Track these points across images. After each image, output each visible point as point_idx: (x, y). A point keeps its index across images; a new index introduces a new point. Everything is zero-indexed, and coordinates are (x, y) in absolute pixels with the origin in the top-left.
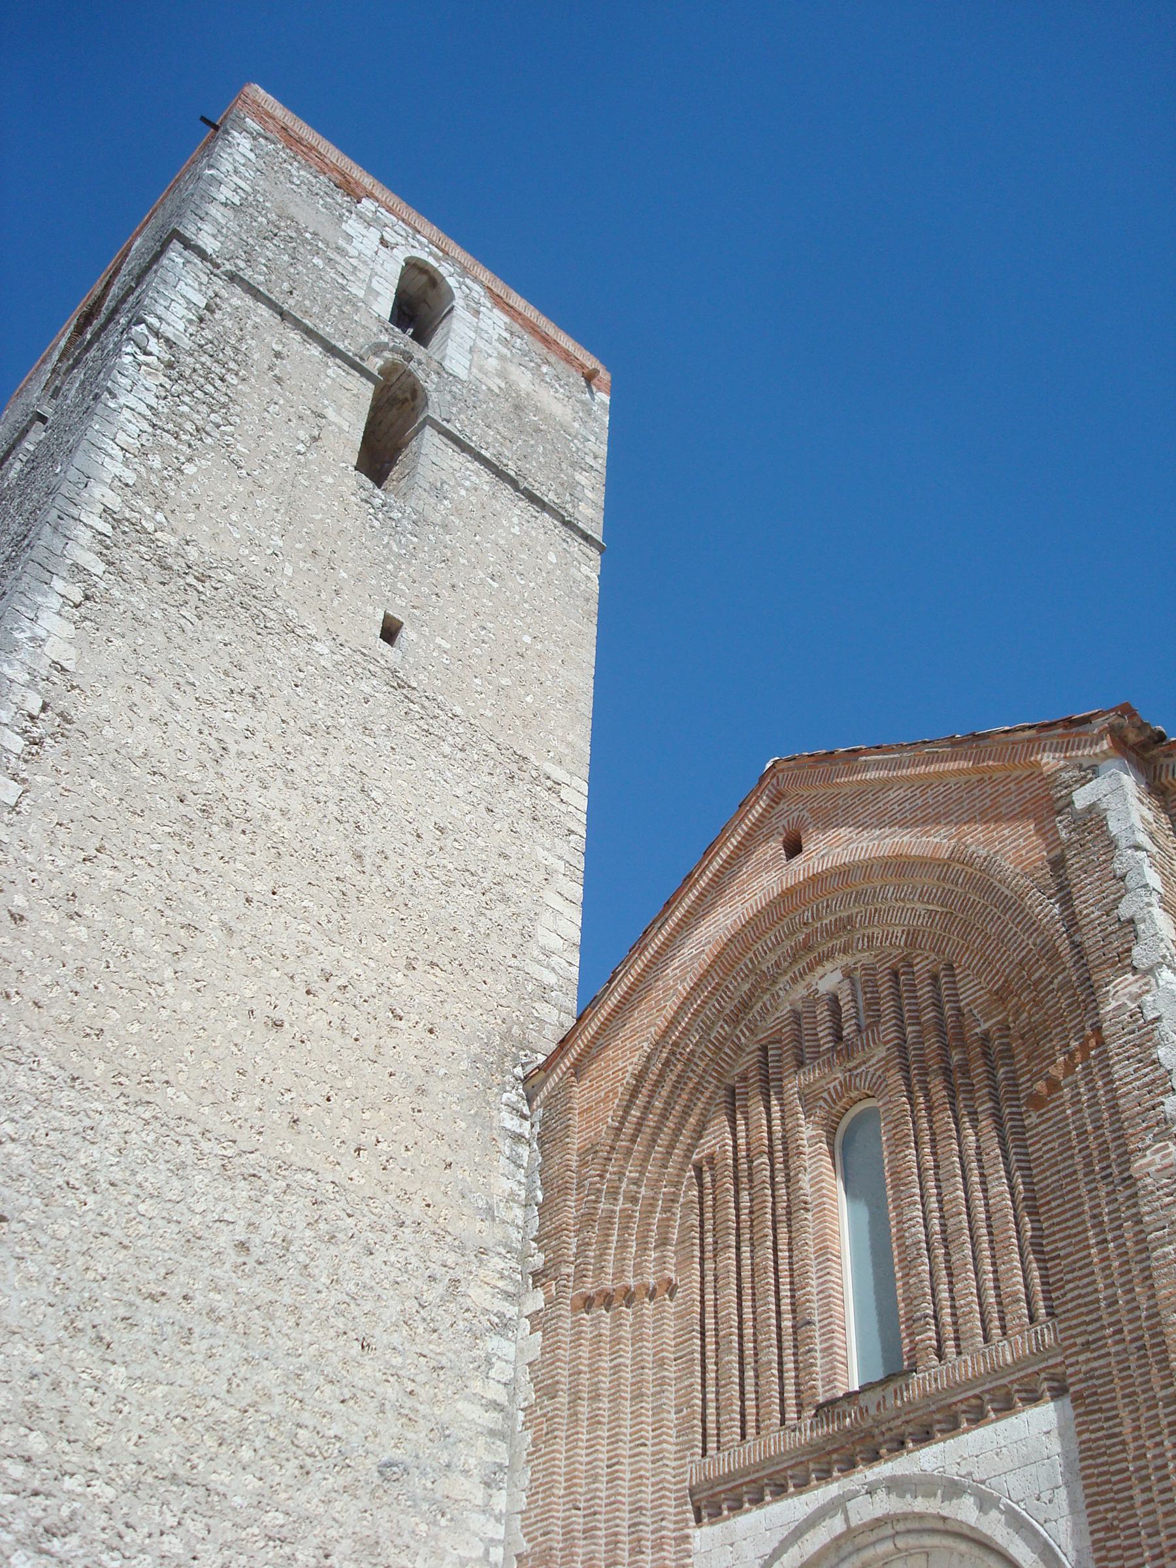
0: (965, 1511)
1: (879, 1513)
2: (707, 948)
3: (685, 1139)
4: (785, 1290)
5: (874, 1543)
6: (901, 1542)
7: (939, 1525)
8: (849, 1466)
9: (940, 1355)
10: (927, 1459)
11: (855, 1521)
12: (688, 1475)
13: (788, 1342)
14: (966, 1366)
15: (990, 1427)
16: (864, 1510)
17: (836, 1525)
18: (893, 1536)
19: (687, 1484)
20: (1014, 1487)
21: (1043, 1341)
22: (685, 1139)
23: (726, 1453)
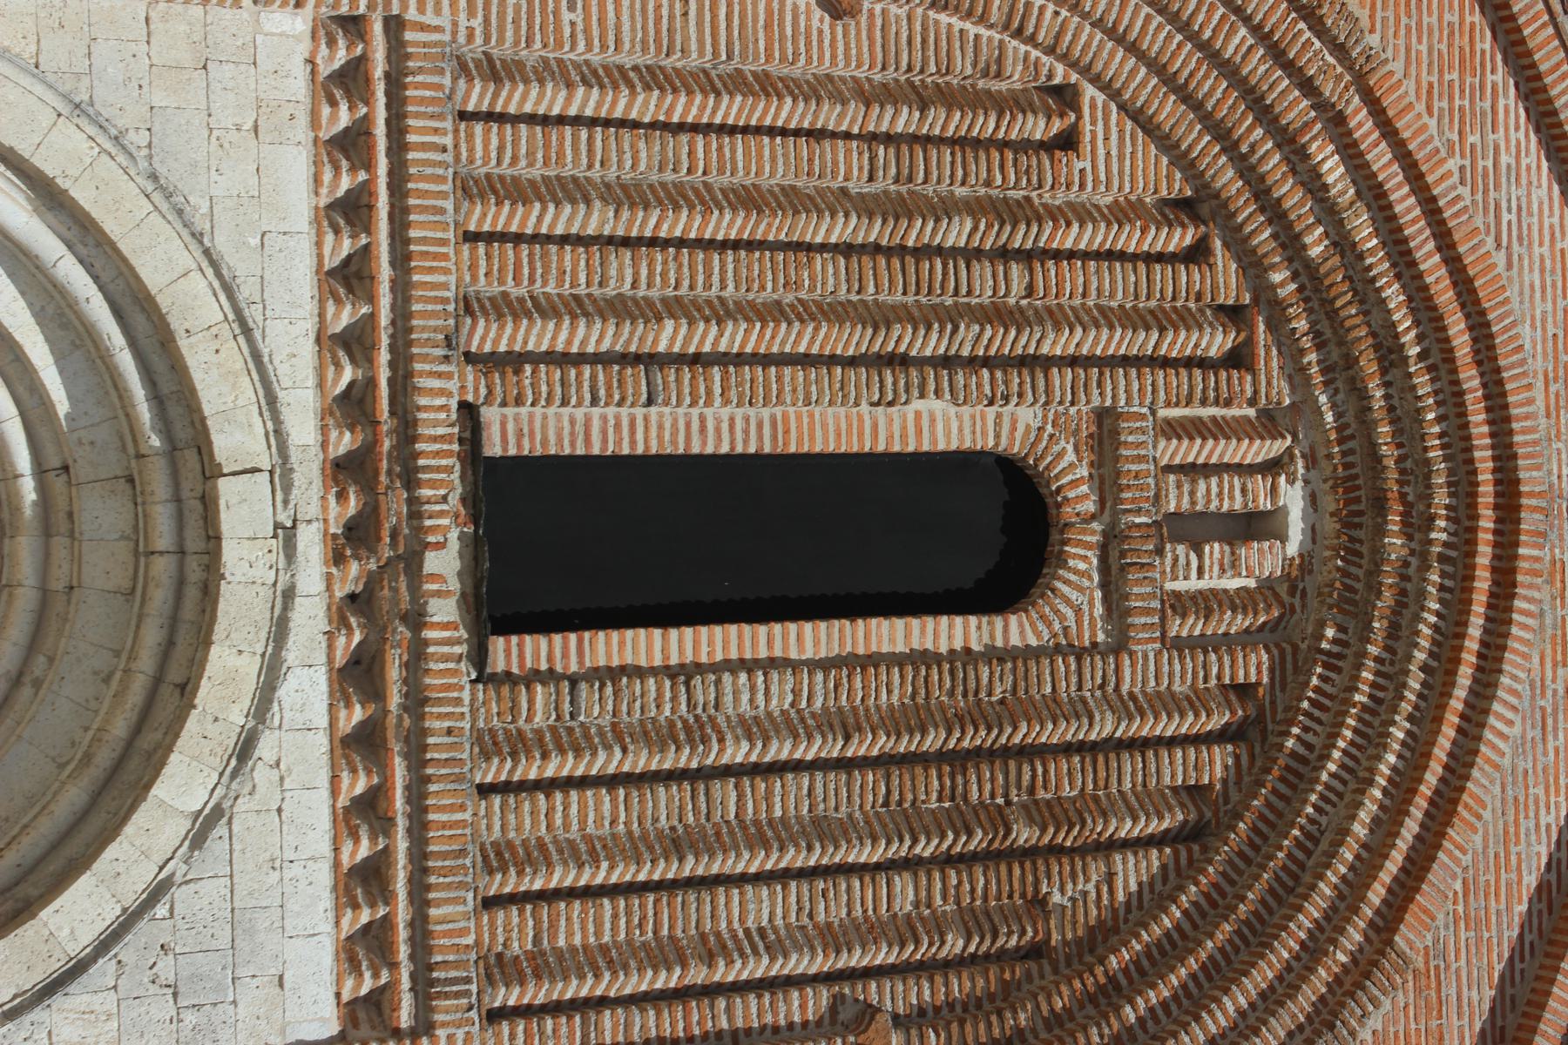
0: (183, 784)
1: (231, 553)
2: (1500, 258)
3: (1142, 85)
4: (734, 337)
5: (177, 499)
6: (163, 568)
7: (175, 675)
8: (346, 471)
9: (487, 745)
10: (307, 690)
11: (227, 489)
12: (429, 18)
13: (630, 337)
14: (451, 808)
15: (325, 848)
16: (244, 510)
17: (236, 437)
18: (182, 552)
19: (412, 14)
20: (201, 899)
21: (447, 996)
22: (1142, 85)
23: (448, 141)
